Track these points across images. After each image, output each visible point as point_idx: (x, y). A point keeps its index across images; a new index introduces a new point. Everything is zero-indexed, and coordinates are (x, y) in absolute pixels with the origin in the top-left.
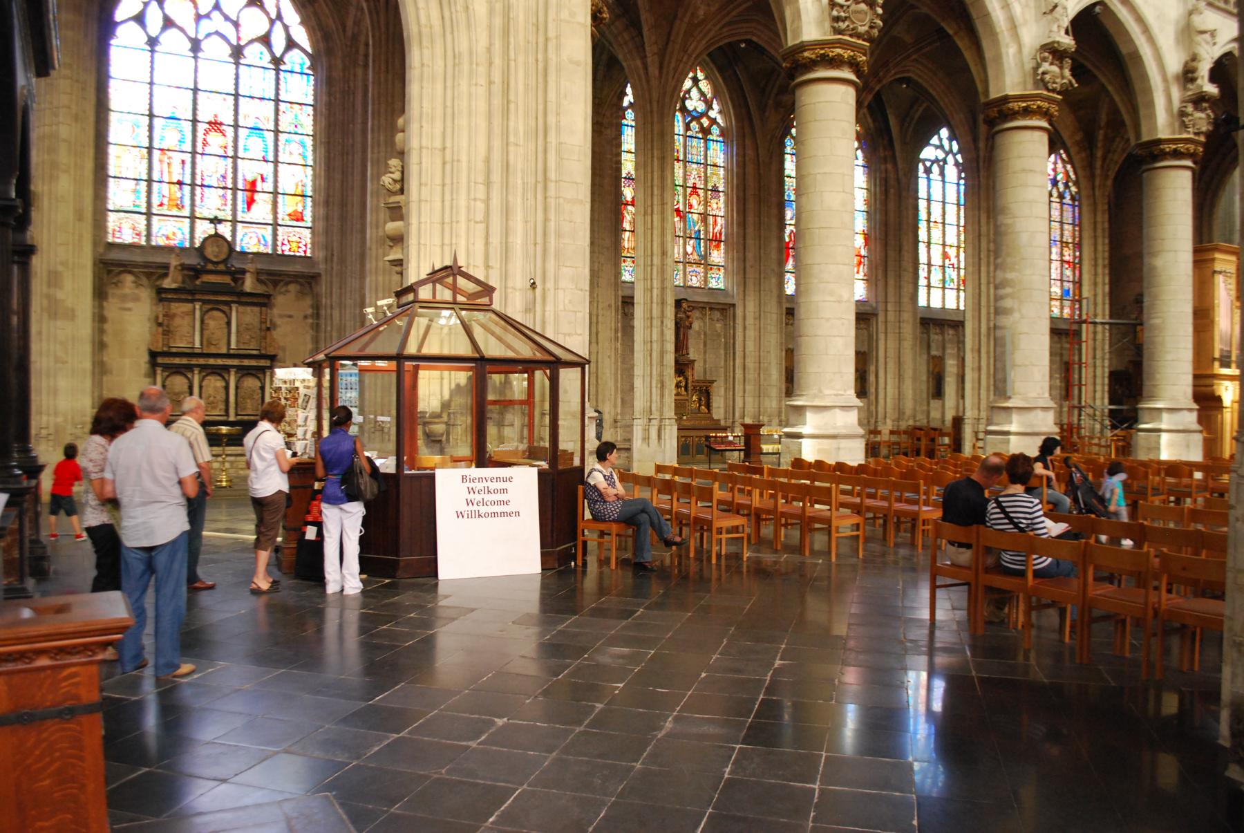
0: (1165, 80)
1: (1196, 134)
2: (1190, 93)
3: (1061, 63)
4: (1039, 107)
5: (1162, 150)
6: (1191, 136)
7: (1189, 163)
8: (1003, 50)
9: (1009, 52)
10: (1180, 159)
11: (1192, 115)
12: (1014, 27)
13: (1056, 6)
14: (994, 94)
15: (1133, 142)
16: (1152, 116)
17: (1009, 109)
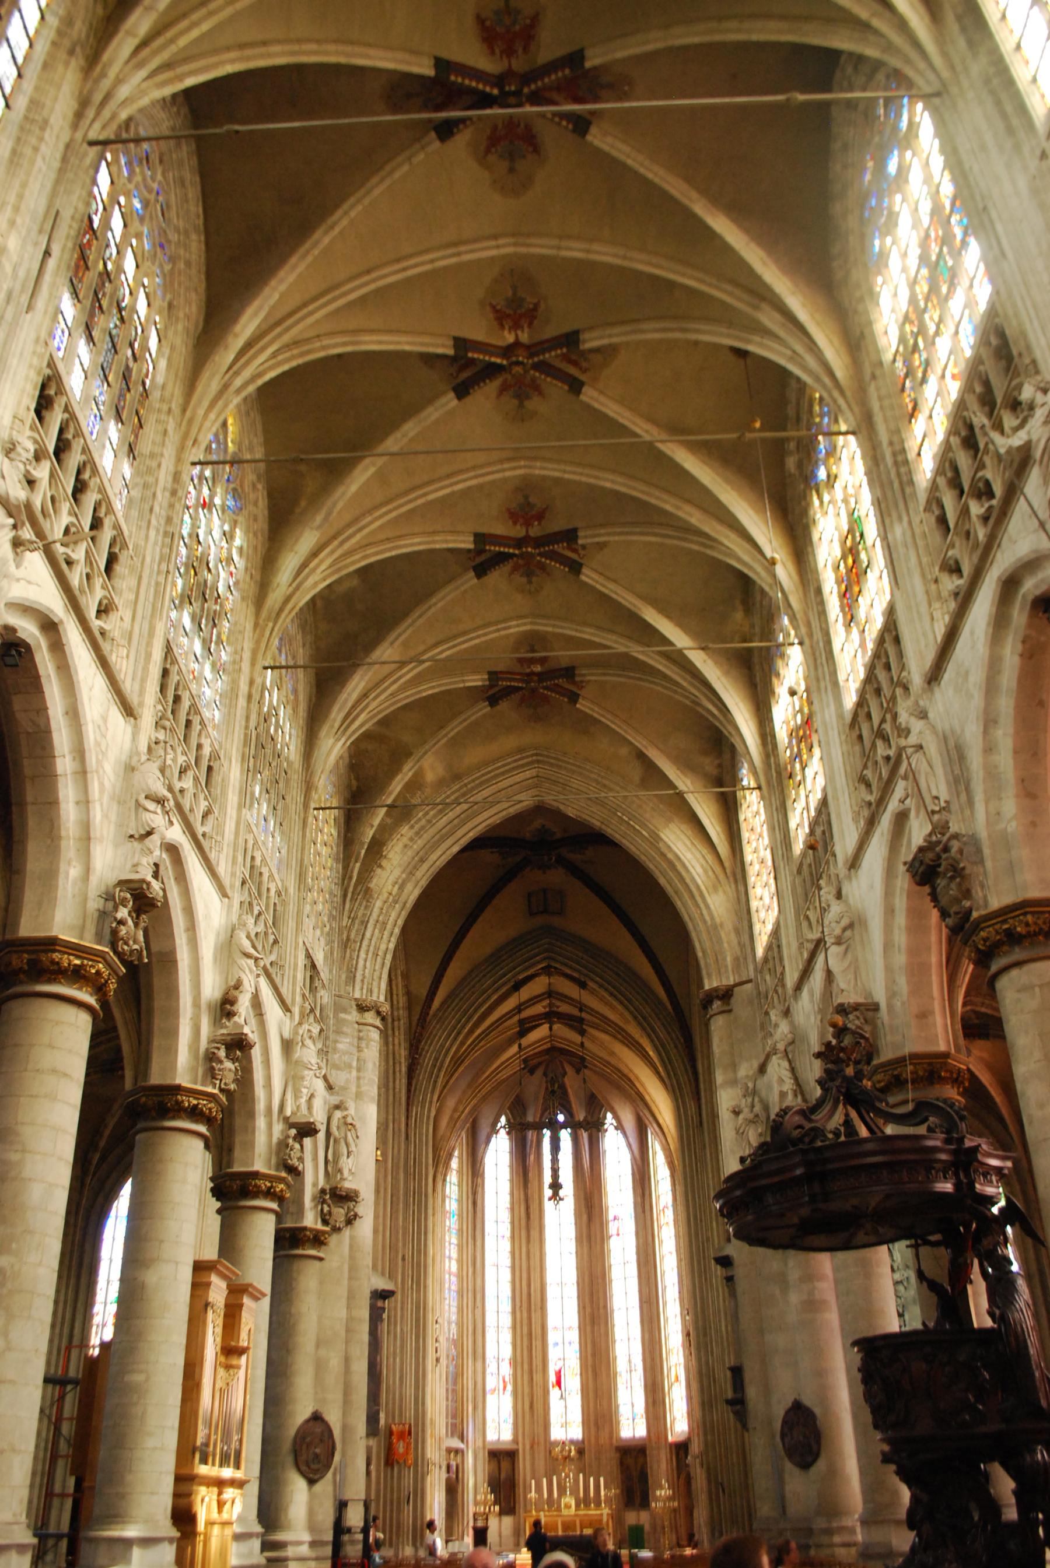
1: (221, 1090)
2: (224, 1031)
3: (138, 917)
4: (98, 973)
5: (179, 1103)
6: (216, 1091)
7: (202, 1129)
8: (63, 867)
9: (70, 872)
10: (196, 1122)
11: (221, 1062)
12: (86, 838)
13: (149, 833)
14: (27, 928)
15: (128, 1085)
16: (171, 1050)
17: (53, 962)
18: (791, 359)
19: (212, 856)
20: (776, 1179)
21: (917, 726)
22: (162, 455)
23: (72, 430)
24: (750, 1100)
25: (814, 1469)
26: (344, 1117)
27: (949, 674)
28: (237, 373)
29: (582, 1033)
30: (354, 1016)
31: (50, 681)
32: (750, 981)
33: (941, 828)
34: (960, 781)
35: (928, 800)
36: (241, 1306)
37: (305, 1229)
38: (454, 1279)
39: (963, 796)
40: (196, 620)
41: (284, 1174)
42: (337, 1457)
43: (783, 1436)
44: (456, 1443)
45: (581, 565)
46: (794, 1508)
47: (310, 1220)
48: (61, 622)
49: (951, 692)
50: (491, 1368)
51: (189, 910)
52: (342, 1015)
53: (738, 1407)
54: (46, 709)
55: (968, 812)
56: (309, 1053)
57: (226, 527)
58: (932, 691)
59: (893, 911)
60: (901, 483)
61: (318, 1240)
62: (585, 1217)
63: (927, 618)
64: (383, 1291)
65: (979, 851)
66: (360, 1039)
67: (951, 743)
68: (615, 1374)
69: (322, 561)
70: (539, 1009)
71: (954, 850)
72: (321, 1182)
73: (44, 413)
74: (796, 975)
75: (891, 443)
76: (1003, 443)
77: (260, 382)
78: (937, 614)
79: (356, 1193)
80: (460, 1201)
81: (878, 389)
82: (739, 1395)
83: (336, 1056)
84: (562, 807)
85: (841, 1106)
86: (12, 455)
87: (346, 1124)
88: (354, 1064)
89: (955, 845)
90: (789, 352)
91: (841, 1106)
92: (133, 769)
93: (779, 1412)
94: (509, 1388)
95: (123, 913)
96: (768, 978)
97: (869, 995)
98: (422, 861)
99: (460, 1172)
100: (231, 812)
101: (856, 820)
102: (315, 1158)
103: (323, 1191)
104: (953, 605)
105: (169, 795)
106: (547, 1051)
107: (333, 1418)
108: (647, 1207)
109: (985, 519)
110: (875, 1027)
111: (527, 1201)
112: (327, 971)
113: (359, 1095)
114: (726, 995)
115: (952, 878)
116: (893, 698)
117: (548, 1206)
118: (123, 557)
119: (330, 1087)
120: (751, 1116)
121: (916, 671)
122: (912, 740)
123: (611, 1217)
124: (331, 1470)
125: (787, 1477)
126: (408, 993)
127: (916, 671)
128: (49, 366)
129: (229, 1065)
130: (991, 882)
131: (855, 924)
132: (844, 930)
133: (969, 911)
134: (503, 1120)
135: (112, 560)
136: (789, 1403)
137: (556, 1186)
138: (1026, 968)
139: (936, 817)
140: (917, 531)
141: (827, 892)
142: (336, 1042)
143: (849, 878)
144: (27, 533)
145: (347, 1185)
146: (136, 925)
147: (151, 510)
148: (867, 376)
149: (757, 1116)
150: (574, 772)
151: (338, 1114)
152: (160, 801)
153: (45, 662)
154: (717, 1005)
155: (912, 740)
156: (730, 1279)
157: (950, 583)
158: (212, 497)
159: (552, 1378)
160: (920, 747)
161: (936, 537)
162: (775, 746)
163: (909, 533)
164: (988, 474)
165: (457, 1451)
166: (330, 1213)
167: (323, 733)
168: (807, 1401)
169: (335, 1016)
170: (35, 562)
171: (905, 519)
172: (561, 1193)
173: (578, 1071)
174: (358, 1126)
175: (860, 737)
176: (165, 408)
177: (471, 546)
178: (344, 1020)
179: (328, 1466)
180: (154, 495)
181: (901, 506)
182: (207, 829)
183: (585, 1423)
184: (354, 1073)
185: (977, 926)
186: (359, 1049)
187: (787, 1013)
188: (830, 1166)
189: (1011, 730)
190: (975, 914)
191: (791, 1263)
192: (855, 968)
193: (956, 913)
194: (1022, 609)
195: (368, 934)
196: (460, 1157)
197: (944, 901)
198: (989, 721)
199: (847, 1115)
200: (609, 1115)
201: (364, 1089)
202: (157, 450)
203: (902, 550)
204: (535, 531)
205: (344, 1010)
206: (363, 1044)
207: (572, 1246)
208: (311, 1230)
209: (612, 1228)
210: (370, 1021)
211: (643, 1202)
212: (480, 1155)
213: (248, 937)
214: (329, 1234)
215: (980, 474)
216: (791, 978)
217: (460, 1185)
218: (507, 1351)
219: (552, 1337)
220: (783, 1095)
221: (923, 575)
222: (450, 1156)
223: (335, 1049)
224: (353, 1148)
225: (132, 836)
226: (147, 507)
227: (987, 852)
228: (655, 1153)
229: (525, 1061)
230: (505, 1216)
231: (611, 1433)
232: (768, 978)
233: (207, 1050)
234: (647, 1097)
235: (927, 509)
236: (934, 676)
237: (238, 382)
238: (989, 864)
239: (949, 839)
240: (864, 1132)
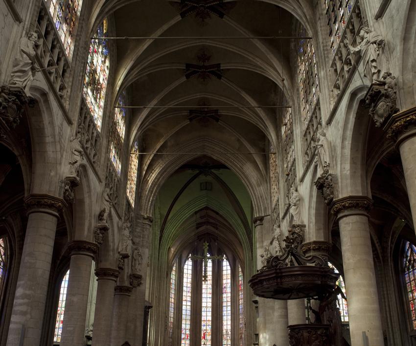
0: (90, 216)
1: (98, 243)
2: (99, 225)
13: (76, 162)
18: (293, 10)
19: (97, 168)
20: (267, 277)
21: (322, 138)
22: (81, 35)
23: (50, 27)
24: (267, 253)
26: (138, 253)
27: (333, 122)
28: (106, 7)
29: (217, 229)
31: (44, 113)
32: (270, 215)
33: (326, 172)
34: (333, 157)
35: (323, 163)
39: (334, 162)
40: (92, 91)
45: (221, 76)
48: (47, 93)
49: (334, 127)
51: (89, 186)
52: (139, 221)
54: (43, 121)
55: (335, 167)
56: (127, 232)
57: (103, 59)
58: (328, 127)
59: (312, 196)
60: (325, 57)
62: (215, 287)
63: (328, 104)
65: (337, 180)
67: (332, 144)
69: (135, 72)
70: (203, 220)
71: (329, 179)
73: (41, 21)
74: (283, 214)
75: (323, 43)
76: (353, 49)
77: (114, 10)
78: (332, 102)
80: (175, 280)
81: (320, 23)
83: (136, 233)
84: (212, 156)
85: (290, 256)
86: (30, 39)
89: (330, 177)
90: (292, 8)
91: (290, 256)
92: (71, 141)
95: (67, 187)
96: (275, 214)
97: (302, 222)
98: (165, 171)
100: (103, 155)
101: (303, 167)
102: (128, 265)
104: (336, 99)
105: (82, 150)
106: (205, 234)
109: (348, 71)
110: (304, 231)
111: (197, 280)
112: (133, 206)
113: (143, 246)
114: (261, 219)
115: (328, 188)
116: (317, 128)
117: (203, 283)
118: (68, 71)
119: (133, 243)
121: (324, 120)
122: (320, 143)
123: (223, 287)
126: (160, 214)
127: (324, 120)
128: (42, 5)
129: (101, 235)
130: (340, 190)
131: (300, 200)
132: (297, 201)
133: (333, 198)
134: (190, 255)
135: (64, 71)
137: (206, 277)
138: (348, 218)
139: (325, 168)
140: (328, 74)
141: (292, 189)
142: (136, 229)
143: (300, 185)
144: (36, 66)
146: (71, 191)
147: (77, 55)
148: (318, 19)
150: (216, 144)
151: (136, 251)
152: (80, 152)
153: (42, 105)
154: (258, 222)
155: (320, 143)
157: (336, 92)
158: (98, 48)
160: (322, 146)
161: (334, 77)
162: (282, 140)
163: (326, 74)
164: (350, 57)
167: (133, 129)
170: (40, 75)
171: (325, 69)
172: (208, 279)
173: (215, 241)
174: (142, 255)
175: (307, 139)
176: (82, 18)
177: (185, 68)
180: (78, 48)
181: (324, 65)
182: (94, 160)
184: (141, 239)
185: (335, 203)
187: (279, 226)
188: (284, 274)
189: (350, 142)
190: (334, 200)
192: (299, 213)
193: (329, 199)
194: (356, 104)
196: (176, 267)
197: (325, 195)
198: (344, 139)
199: (291, 259)
200: (225, 256)
201: (144, 244)
202: (79, 33)
203: (323, 80)
204: (207, 64)
205: (139, 219)
207: (211, 296)
210: (147, 223)
213: (108, 195)
215: (348, 57)
216: (281, 215)
217: (175, 275)
220: (277, 252)
221: (329, 89)
222: (173, 265)
223: (136, 231)
225: (70, 163)
226: (76, 53)
227: (340, 180)
228: (238, 268)
229: (198, 237)
230: (189, 285)
232: (275, 214)
233: (94, 230)
234: (237, 250)
235: (332, 66)
236: (329, 122)
237: (107, 10)
238: (340, 184)
239: (328, 176)
240: (296, 264)
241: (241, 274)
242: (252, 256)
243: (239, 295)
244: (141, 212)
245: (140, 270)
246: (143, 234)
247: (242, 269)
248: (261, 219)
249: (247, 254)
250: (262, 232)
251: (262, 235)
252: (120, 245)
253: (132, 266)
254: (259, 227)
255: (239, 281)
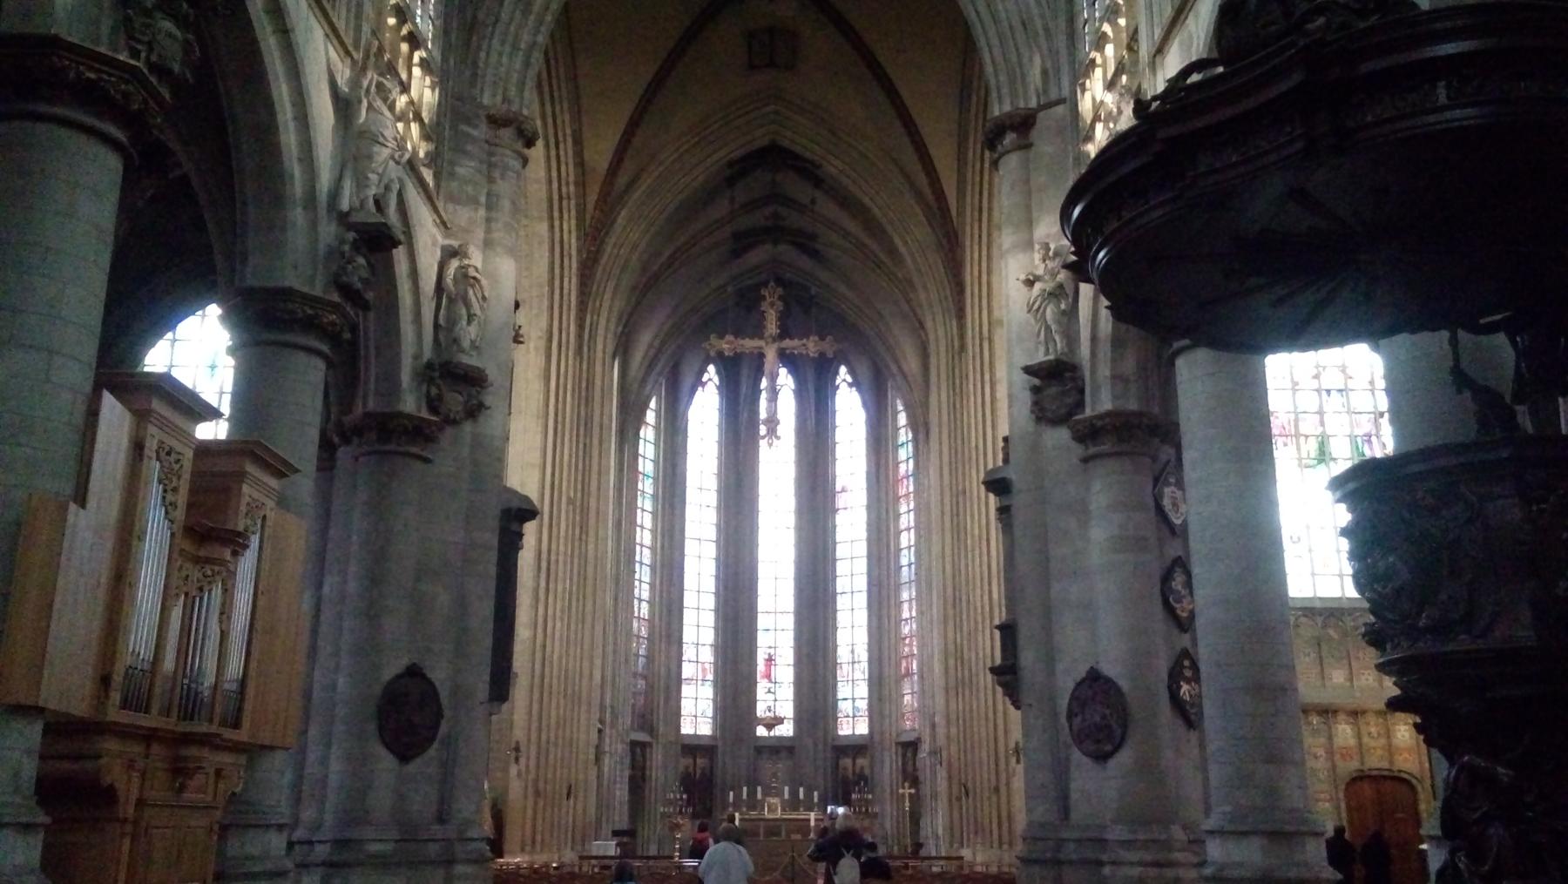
1: (153, 67)
10: (99, 115)
25: (1112, 763)
30: (481, 131)
36: (241, 476)
37: (400, 415)
38: (647, 552)
41: (335, 297)
42: (443, 729)
43: (1071, 715)
44: (642, 737)
46: (1079, 812)
47: (410, 403)
50: (688, 652)
53: (1008, 678)
61: (420, 433)
64: (520, 510)
66: (491, 166)
68: (835, 664)
70: (758, 219)
72: (428, 353)
74: (1158, 33)
79: (480, 371)
82: (1009, 663)
83: (454, 184)
87: (466, 276)
88: (483, 199)
93: (1066, 684)
94: (710, 677)
99: (657, 428)
103: (429, 366)
107: (439, 674)
108: (882, 478)
114: (1024, 123)
117: (763, 443)
120: (1049, 286)
123: (838, 487)
124: (435, 745)
125: (1075, 773)
134: (711, 368)
136: (1081, 671)
137: (772, 422)
142: (452, 163)
145: (465, 359)
149: (1061, 286)
154: (1010, 138)
156: (1004, 511)
159: (761, 667)
165: (643, 745)
166: (440, 397)
168: (1109, 669)
169: (454, 127)
172: (780, 430)
178: (468, 135)
179: (431, 740)
183: (798, 721)
184: (482, 212)
186: (491, 180)
191: (1097, 486)
195: (504, 16)
196: (658, 412)
200: (843, 370)
205: (468, 122)
206: (497, 174)
208: (409, 417)
209: (841, 501)
211: (878, 470)
212: (682, 408)
214: (441, 429)
217: (657, 444)
218: (709, 636)
219: (762, 621)
222: (646, 406)
223: (452, 175)
224: (476, 309)
228: (896, 413)
231: (826, 732)
241: (904, 435)
242: (962, 337)
243: (898, 516)
244: (477, 91)
245: (476, 348)
246: (489, 195)
247: (908, 417)
248: (1024, 123)
249: (941, 332)
250: (1027, 181)
251: (1029, 194)
252: (348, 186)
253: (436, 326)
254: (1012, 162)
255: (897, 464)
